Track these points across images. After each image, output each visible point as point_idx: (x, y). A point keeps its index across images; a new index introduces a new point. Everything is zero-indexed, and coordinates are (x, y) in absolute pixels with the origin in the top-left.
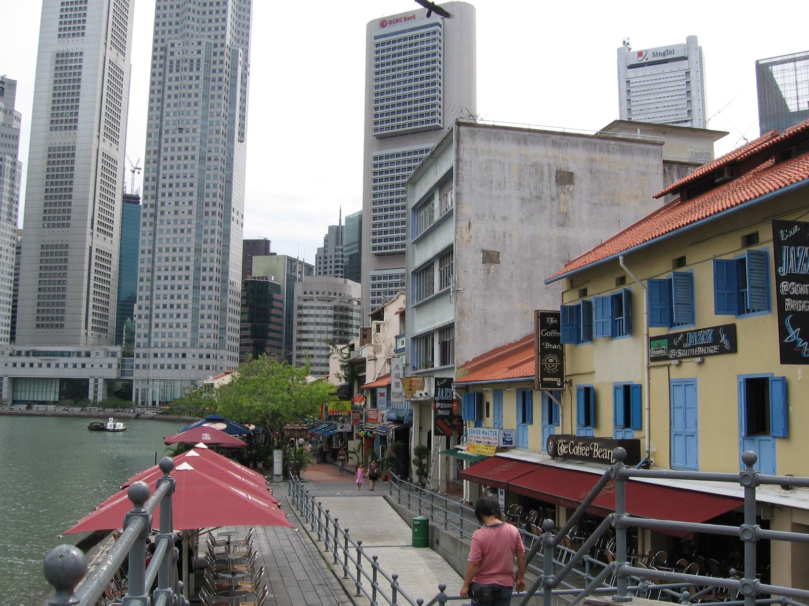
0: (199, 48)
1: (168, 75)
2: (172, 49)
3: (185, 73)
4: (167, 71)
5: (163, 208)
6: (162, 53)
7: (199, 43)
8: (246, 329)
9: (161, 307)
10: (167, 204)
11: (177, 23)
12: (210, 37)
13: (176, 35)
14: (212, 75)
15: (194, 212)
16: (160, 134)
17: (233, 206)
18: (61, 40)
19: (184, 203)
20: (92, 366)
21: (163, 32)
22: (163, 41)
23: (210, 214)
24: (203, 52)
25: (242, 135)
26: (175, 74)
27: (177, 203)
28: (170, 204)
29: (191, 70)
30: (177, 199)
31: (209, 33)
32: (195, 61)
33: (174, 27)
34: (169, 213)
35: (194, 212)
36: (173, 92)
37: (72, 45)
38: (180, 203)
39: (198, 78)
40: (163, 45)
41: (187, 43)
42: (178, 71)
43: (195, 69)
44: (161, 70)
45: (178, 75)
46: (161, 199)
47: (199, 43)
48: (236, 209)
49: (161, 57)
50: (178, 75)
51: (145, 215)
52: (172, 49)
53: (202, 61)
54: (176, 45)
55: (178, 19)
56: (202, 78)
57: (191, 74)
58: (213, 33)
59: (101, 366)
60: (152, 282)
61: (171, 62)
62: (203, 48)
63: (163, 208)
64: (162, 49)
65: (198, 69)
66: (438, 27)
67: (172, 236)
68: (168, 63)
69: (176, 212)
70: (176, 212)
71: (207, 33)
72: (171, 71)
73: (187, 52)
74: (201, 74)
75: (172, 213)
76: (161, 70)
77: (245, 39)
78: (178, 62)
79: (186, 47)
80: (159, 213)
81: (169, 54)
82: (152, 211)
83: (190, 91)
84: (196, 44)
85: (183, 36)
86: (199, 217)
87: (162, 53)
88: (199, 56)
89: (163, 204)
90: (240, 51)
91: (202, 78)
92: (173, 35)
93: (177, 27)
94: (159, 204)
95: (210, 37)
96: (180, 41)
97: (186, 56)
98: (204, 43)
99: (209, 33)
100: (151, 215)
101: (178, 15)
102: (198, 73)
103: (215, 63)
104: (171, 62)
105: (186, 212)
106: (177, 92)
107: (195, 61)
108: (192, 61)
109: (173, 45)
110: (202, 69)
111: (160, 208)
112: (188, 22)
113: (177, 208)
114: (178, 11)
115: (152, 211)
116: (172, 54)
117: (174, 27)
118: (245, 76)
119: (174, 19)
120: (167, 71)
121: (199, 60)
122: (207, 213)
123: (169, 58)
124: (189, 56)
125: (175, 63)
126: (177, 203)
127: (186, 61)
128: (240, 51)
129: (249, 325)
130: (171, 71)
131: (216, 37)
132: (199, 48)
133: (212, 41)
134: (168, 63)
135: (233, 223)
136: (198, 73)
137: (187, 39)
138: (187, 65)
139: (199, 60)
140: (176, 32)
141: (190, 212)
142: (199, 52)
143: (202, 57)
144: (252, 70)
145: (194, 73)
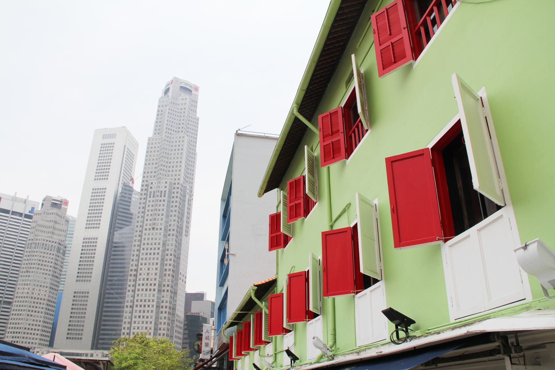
0: (166, 185)
1: (148, 199)
2: (152, 186)
3: (157, 198)
4: (148, 197)
5: (141, 272)
6: (146, 187)
7: (166, 183)
8: (186, 343)
9: (136, 328)
11: (155, 172)
12: (172, 179)
13: (154, 178)
14: (172, 200)
15: (158, 274)
17: (180, 271)
18: (96, 181)
21: (147, 177)
22: (147, 181)
23: (167, 275)
24: (168, 187)
25: (187, 232)
26: (152, 199)
27: (149, 269)
29: (161, 196)
30: (149, 267)
31: (172, 177)
32: (163, 192)
33: (153, 174)
35: (158, 274)
36: (151, 208)
37: (101, 184)
38: (151, 269)
39: (164, 201)
40: (147, 183)
41: (160, 182)
42: (154, 197)
43: (163, 196)
44: (145, 196)
45: (153, 199)
46: (140, 266)
47: (166, 183)
48: (182, 273)
49: (146, 190)
50: (153, 199)
52: (152, 186)
53: (167, 192)
54: (154, 183)
55: (156, 170)
56: (166, 201)
57: (160, 199)
58: (174, 177)
60: (132, 314)
61: (151, 192)
62: (167, 185)
63: (141, 272)
64: (146, 185)
65: (165, 196)
68: (149, 193)
69: (148, 274)
70: (148, 274)
71: (170, 177)
72: (150, 197)
73: (159, 187)
74: (166, 199)
76: (145, 196)
77: (191, 181)
78: (154, 192)
79: (159, 185)
83: (159, 208)
84: (164, 183)
85: (158, 179)
86: (161, 277)
87: (146, 187)
88: (165, 189)
89: (141, 269)
90: (188, 187)
91: (166, 201)
92: (153, 178)
93: (155, 174)
95: (172, 179)
96: (156, 181)
97: (158, 189)
98: (168, 183)
99: (172, 177)
100: (134, 275)
101: (155, 168)
102: (164, 198)
103: (174, 193)
104: (151, 192)
105: (154, 274)
106: (153, 208)
107: (163, 192)
108: (162, 192)
109: (152, 183)
110: (167, 196)
111: (139, 272)
112: (161, 171)
114: (156, 166)
115: (135, 273)
116: (151, 188)
117: (153, 174)
118: (190, 200)
119: (154, 170)
120: (148, 197)
121: (165, 191)
122: (165, 275)
123: (150, 190)
124: (161, 189)
125: (152, 192)
126: (149, 269)
127: (158, 192)
128: (188, 187)
129: (188, 341)
130: (150, 197)
131: (175, 179)
132: (166, 185)
133: (173, 181)
134: (149, 193)
135: (180, 281)
136: (164, 198)
137: (160, 180)
138: (159, 194)
139: (165, 191)
140: (154, 176)
141: (156, 274)
142: (166, 187)
143: (167, 189)
144: (194, 197)
145: (162, 198)
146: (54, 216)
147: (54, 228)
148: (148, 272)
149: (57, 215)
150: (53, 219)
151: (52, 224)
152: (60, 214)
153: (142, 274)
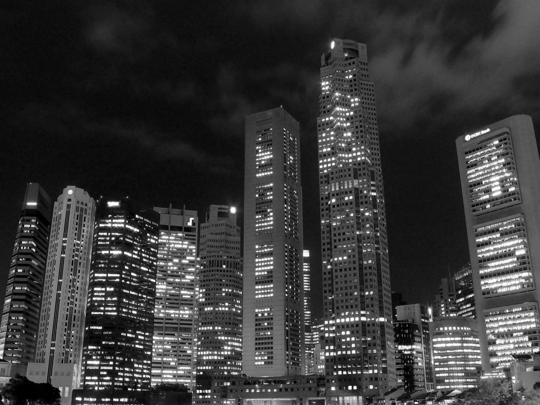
0: (350, 172)
5: (337, 280)
10: (339, 277)
16: (330, 231)
19: (350, 275)
20: (298, 389)
27: (346, 276)
28: (341, 276)
30: (346, 273)
34: (341, 282)
38: (348, 275)
51: (325, 285)
52: (332, 176)
59: (304, 389)
63: (337, 280)
66: (506, 135)
67: (344, 298)
69: (346, 282)
70: (346, 282)
75: (343, 282)
80: (334, 283)
81: (330, 179)
82: (330, 282)
89: (337, 277)
94: (334, 277)
111: (335, 280)
113: (346, 279)
115: (330, 282)
126: (346, 276)
146: (223, 227)
147: (226, 241)
148: (346, 279)
149: (227, 225)
150: (224, 231)
151: (223, 237)
152: (229, 223)
153: (339, 283)
